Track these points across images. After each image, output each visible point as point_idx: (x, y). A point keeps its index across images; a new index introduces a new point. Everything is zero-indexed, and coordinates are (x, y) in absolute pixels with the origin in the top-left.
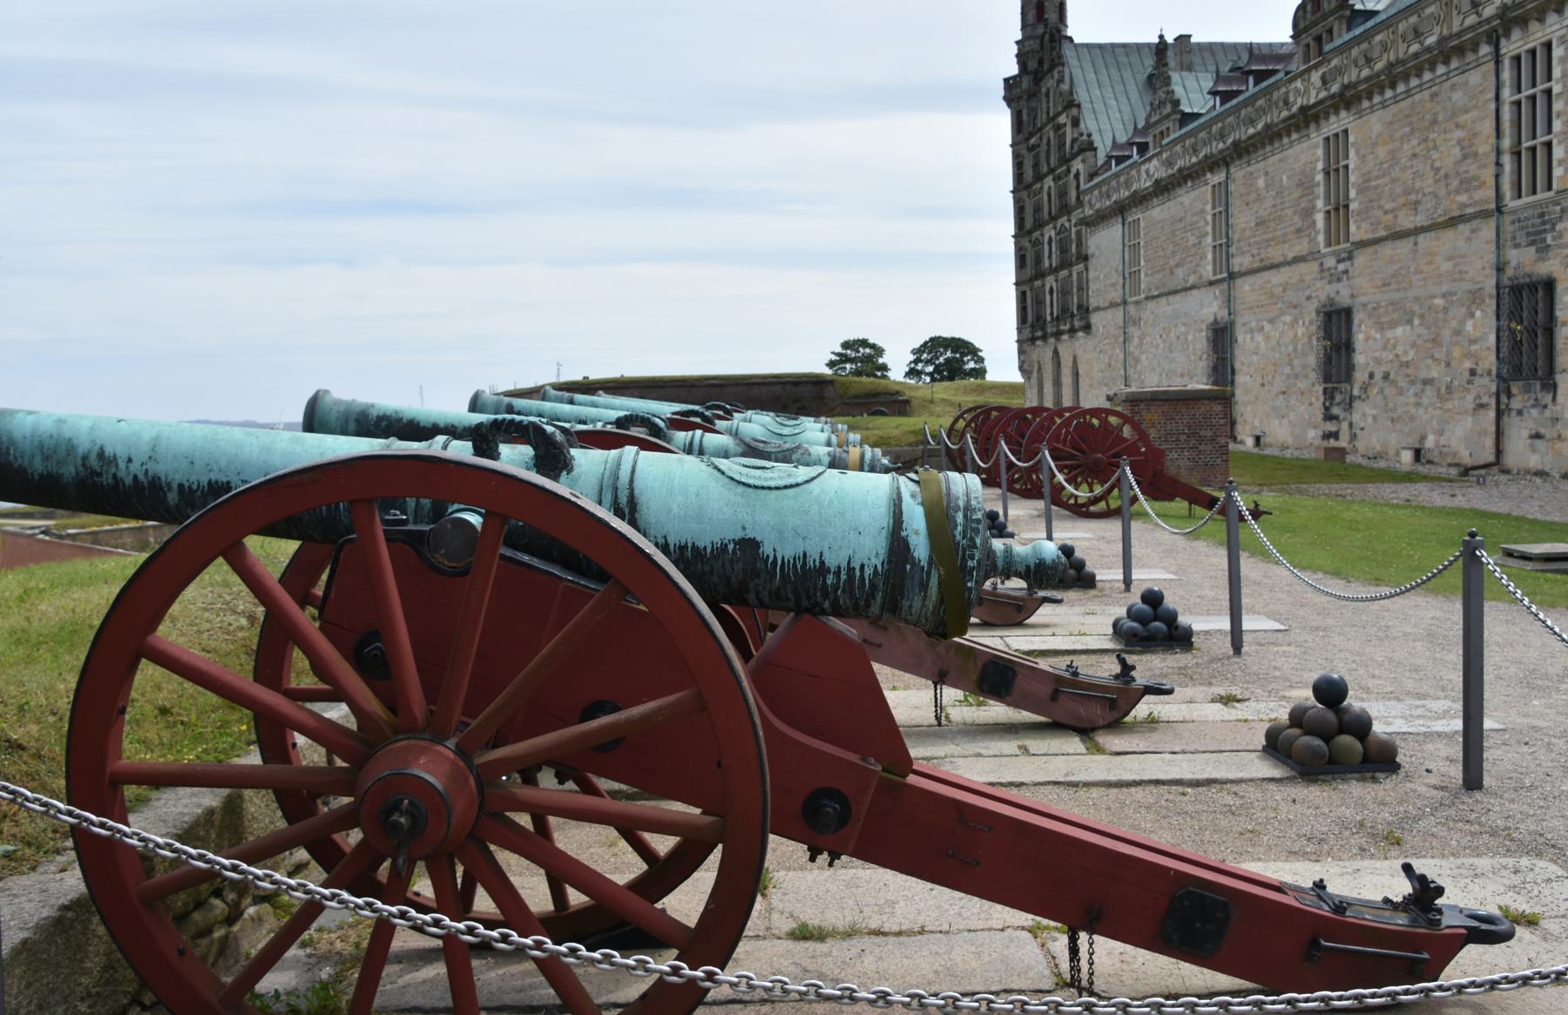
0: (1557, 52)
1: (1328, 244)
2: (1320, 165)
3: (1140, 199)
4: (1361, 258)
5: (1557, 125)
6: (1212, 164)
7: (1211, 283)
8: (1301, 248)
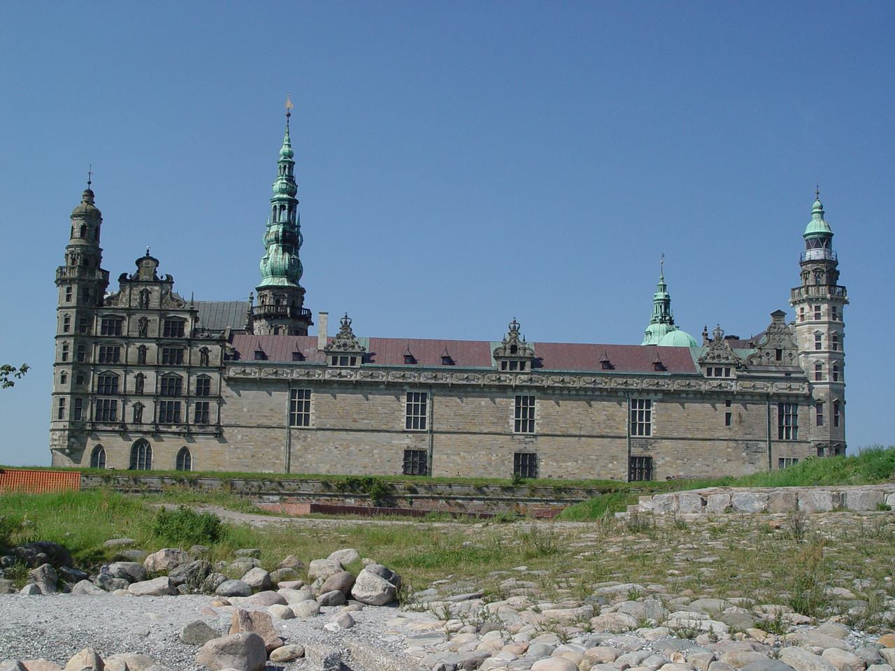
4: (540, 439)
7: (404, 432)
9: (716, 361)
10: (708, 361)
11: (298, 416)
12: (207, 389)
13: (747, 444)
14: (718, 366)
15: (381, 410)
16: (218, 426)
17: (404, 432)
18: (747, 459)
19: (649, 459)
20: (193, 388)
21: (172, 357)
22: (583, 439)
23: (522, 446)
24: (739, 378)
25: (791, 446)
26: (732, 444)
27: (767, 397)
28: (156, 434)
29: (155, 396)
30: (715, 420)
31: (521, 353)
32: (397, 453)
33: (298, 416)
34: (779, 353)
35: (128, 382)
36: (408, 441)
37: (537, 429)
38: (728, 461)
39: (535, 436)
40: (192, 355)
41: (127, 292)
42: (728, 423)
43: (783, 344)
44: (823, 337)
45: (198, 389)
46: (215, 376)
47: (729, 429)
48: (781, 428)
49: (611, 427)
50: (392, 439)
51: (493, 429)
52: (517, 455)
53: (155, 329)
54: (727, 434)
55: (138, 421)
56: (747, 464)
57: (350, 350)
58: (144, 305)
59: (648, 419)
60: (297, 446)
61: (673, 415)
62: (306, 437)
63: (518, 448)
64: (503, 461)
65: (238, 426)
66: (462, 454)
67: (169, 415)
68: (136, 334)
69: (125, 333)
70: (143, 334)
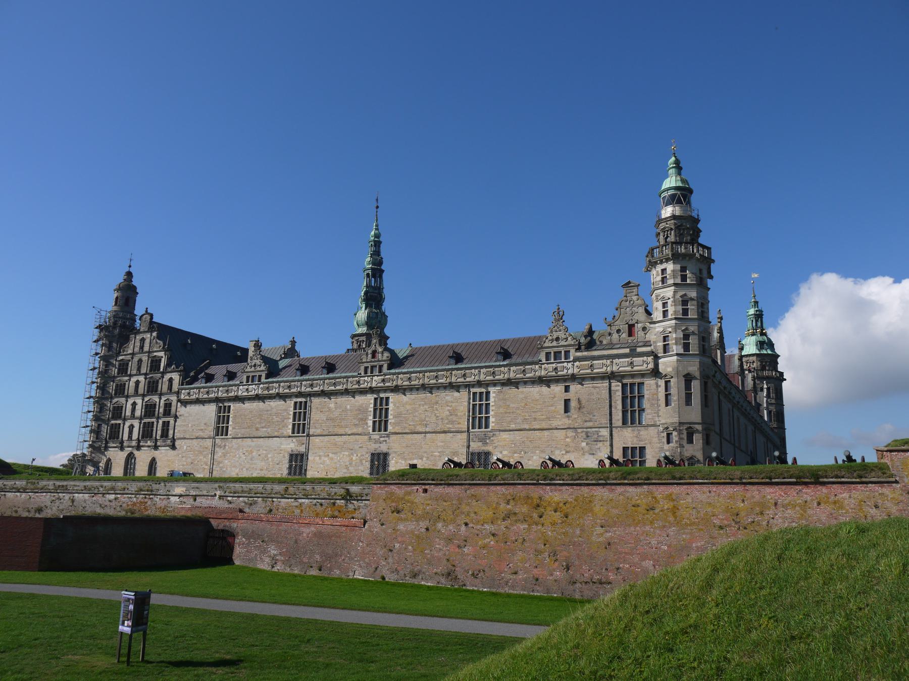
0: (492, 395)
1: (374, 430)
2: (372, 406)
3: (237, 399)
4: (393, 437)
5: (492, 413)
6: (300, 394)
7: (290, 437)
8: (360, 430)
9: (555, 344)
13: (587, 433)
14: (556, 349)
15: (275, 419)
17: (290, 437)
18: (587, 448)
25: (636, 433)
26: (571, 433)
28: (138, 448)
29: (141, 419)
30: (553, 408)
32: (284, 457)
34: (631, 327)
36: (293, 445)
37: (390, 428)
38: (567, 452)
39: (388, 436)
42: (567, 409)
43: (636, 317)
44: (670, 302)
45: (165, 410)
47: (568, 417)
48: (624, 412)
49: (452, 422)
51: (355, 430)
54: (566, 422)
55: (130, 437)
56: (587, 456)
59: (487, 412)
60: (219, 452)
61: (511, 405)
63: (373, 447)
64: (361, 461)
65: (185, 438)
66: (331, 455)
67: (147, 432)
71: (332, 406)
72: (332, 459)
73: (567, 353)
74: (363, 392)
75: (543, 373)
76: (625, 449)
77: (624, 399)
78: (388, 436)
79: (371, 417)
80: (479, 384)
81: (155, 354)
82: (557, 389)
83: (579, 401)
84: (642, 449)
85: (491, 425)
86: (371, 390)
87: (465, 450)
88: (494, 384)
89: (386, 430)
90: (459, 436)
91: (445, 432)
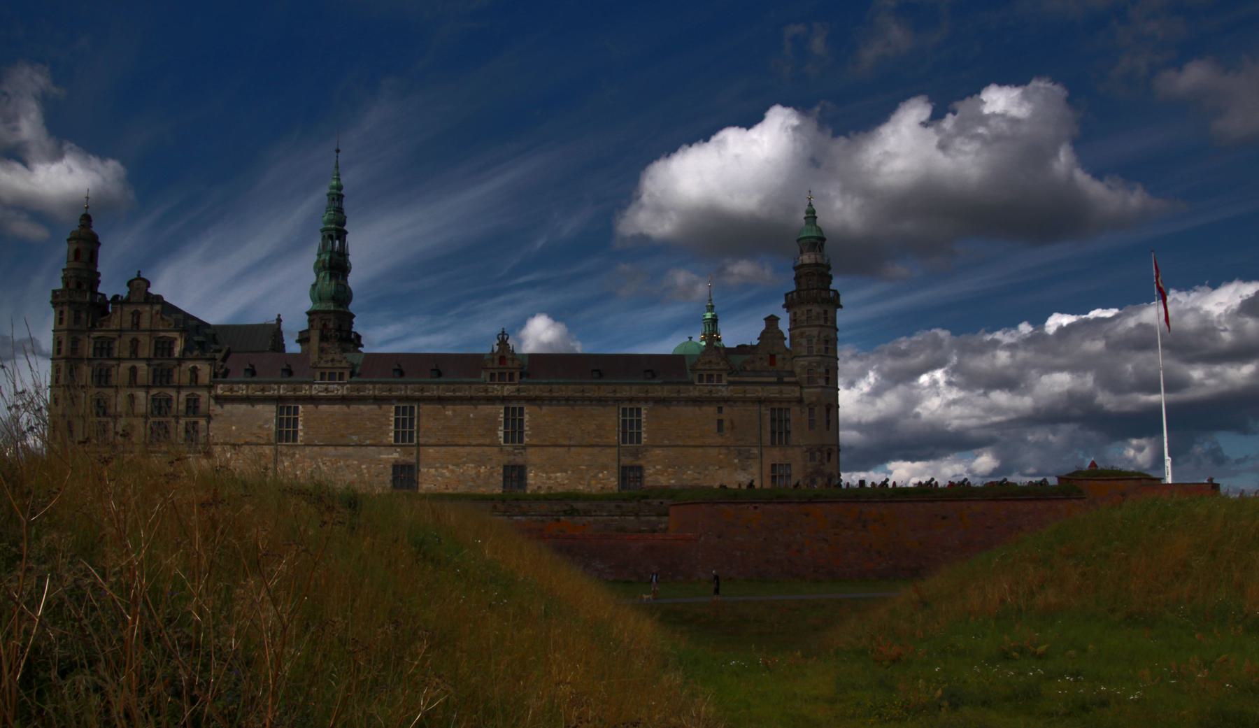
0: (643, 412)
4: (530, 450)
8: (488, 441)
9: (707, 367)
10: (699, 367)
11: (286, 433)
12: (196, 407)
15: (369, 425)
16: (207, 443)
19: (640, 468)
20: (182, 407)
21: (162, 377)
22: (573, 449)
23: (512, 457)
24: (730, 383)
26: (724, 451)
27: (760, 401)
29: (146, 417)
31: (509, 363)
33: (286, 433)
35: (119, 402)
37: (526, 440)
38: (721, 468)
40: (182, 374)
41: (119, 314)
45: (188, 407)
46: (203, 394)
48: (773, 433)
50: (380, 453)
51: (481, 441)
52: (505, 467)
53: (146, 351)
57: (338, 365)
58: (136, 325)
62: (294, 454)
63: (506, 460)
68: (126, 354)
69: (116, 355)
70: (134, 355)
71: (450, 413)
72: (453, 471)
73: (720, 376)
74: (491, 400)
75: (697, 394)
76: (774, 466)
77: (773, 420)
78: (524, 448)
79: (502, 428)
80: (631, 400)
81: (162, 334)
82: (711, 410)
83: (732, 423)
84: (789, 465)
85: (644, 440)
86: (503, 399)
87: (616, 465)
88: (646, 400)
89: (521, 440)
90: (608, 450)
91: (592, 446)
